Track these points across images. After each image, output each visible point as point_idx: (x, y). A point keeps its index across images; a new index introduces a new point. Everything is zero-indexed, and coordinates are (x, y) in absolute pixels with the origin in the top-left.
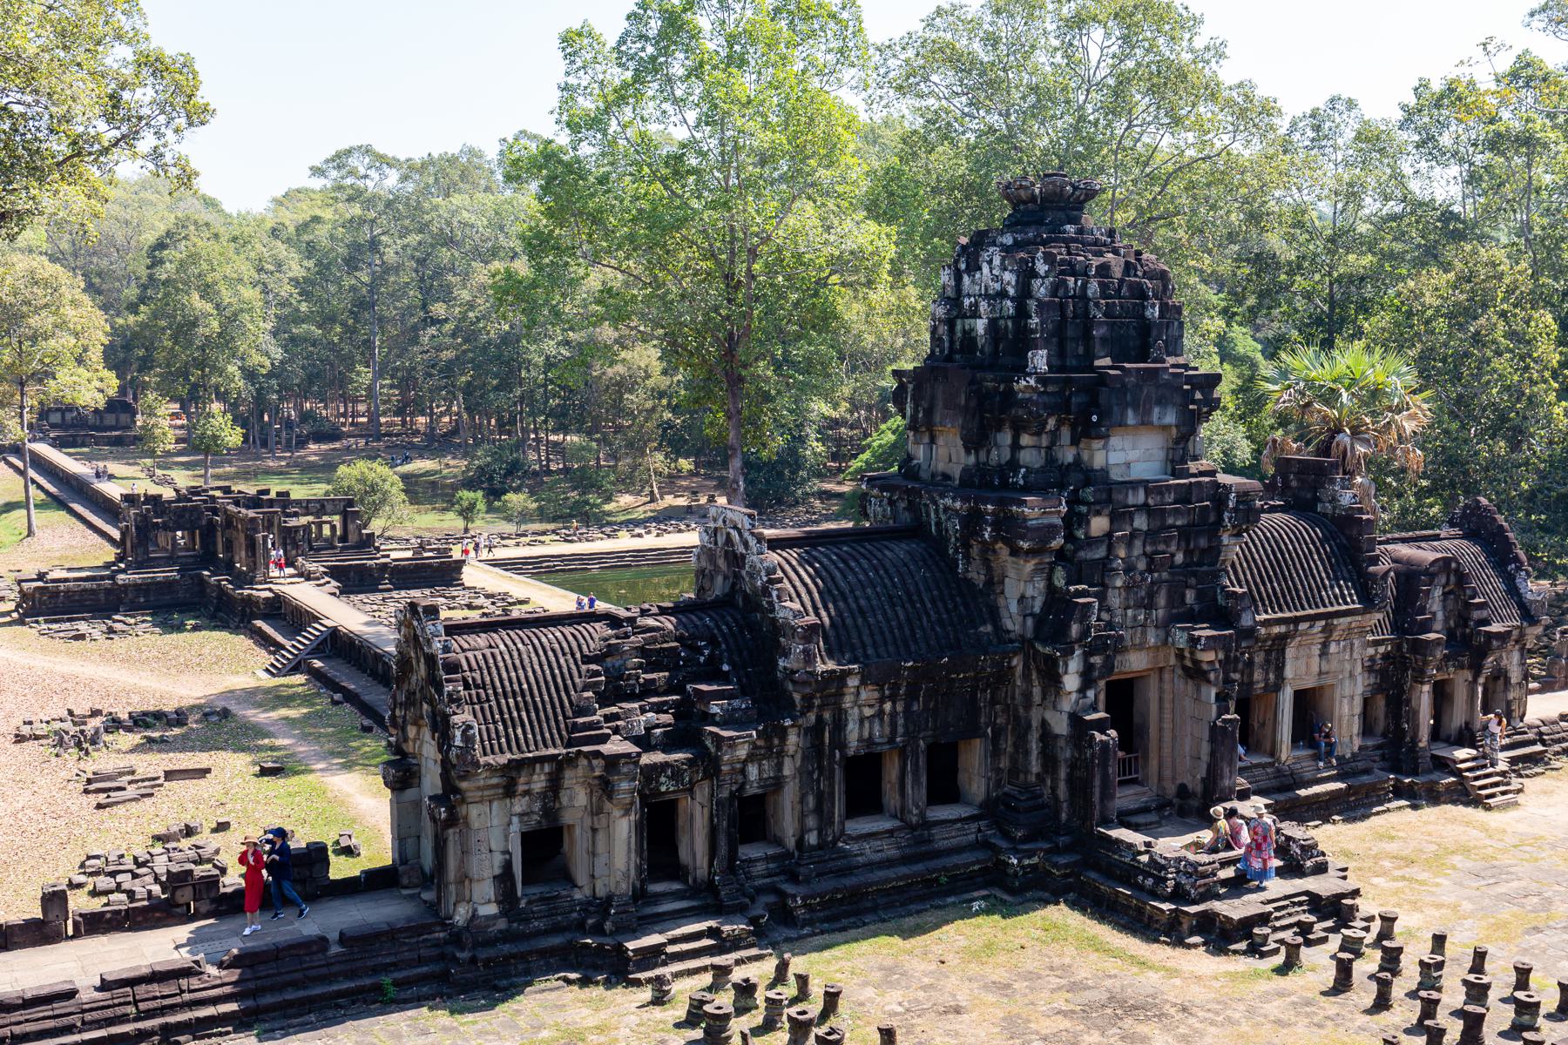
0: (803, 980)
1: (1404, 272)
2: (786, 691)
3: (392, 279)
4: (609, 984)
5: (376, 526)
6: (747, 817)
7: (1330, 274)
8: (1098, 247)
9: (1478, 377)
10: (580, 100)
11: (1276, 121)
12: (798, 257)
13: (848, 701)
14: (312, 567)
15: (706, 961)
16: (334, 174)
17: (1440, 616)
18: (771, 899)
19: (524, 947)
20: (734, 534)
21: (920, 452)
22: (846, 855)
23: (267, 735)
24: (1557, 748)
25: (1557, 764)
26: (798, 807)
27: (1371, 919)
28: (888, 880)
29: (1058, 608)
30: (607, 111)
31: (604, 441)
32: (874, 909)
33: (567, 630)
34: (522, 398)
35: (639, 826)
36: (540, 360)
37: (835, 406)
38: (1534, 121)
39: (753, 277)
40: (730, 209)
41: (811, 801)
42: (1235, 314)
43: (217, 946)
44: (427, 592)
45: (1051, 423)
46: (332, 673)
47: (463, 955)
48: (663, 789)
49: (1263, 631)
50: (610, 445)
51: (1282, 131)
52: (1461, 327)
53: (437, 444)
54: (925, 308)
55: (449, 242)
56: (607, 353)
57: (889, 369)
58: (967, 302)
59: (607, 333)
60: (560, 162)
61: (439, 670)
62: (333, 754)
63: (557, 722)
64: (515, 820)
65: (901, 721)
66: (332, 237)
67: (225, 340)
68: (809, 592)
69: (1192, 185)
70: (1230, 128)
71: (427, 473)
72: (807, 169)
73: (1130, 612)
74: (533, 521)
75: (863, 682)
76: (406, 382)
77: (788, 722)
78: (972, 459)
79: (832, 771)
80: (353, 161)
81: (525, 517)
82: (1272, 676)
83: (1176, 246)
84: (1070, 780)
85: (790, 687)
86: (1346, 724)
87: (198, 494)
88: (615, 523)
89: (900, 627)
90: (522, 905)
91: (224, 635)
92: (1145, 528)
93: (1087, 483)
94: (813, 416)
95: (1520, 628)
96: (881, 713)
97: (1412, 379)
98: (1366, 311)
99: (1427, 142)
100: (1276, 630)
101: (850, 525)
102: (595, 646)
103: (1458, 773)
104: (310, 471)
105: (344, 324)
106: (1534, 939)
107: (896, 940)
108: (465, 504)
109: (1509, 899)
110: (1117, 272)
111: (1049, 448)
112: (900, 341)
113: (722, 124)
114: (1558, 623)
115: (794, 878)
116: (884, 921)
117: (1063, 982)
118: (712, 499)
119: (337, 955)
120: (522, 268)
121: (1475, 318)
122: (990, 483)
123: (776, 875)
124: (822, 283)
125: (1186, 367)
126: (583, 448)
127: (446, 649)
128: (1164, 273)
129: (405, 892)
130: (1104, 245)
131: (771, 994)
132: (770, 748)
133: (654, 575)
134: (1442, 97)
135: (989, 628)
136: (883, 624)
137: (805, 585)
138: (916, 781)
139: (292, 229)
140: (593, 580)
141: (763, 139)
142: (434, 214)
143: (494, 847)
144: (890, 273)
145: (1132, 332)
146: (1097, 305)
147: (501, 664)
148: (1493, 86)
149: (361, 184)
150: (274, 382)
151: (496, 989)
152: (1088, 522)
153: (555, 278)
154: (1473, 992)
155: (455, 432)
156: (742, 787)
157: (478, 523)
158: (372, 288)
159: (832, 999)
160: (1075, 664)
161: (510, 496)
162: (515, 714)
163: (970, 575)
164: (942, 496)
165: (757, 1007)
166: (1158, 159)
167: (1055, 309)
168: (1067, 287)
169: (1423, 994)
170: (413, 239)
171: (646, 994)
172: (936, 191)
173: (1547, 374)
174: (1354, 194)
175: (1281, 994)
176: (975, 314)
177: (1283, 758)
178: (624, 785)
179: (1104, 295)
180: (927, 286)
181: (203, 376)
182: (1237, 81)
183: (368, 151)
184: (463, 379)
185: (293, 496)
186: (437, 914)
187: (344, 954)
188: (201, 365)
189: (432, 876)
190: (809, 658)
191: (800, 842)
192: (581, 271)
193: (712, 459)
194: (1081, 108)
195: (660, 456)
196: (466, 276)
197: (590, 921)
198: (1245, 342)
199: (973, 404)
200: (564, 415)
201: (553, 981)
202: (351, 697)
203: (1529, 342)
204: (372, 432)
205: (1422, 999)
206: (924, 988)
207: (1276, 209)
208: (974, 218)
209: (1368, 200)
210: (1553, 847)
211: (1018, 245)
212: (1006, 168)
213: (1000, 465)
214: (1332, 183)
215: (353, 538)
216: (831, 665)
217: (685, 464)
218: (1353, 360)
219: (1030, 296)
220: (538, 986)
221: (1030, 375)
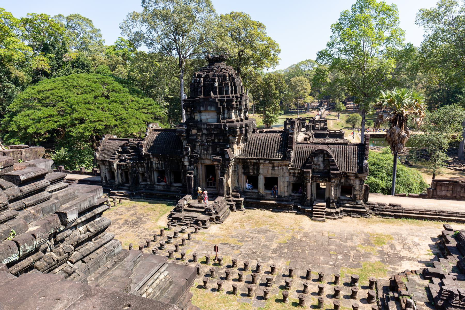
82: (255, 172)
86: (284, 188)
92: (206, 133)
100: (253, 161)
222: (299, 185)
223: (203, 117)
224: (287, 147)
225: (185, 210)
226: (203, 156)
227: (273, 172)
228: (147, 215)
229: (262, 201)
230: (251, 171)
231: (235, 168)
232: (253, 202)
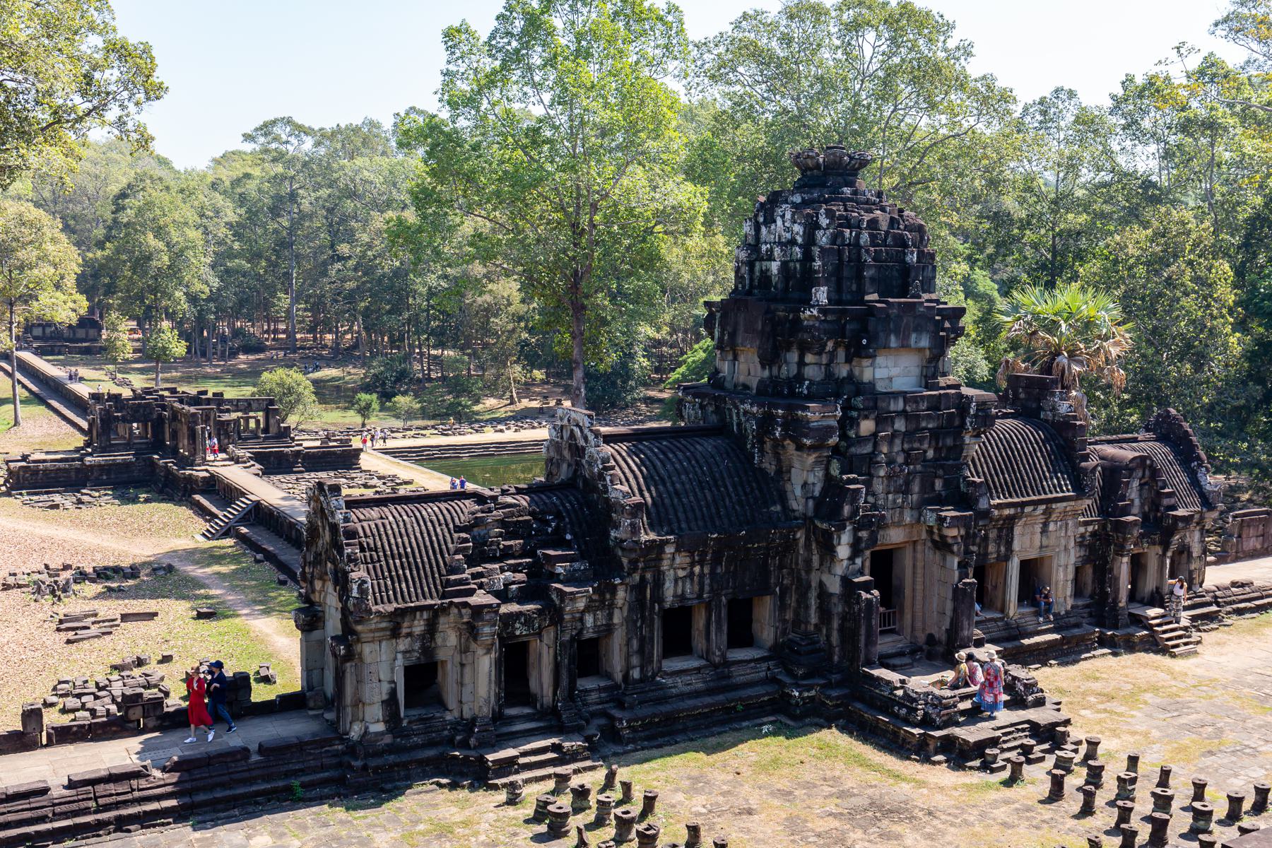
0: (627, 787)
1: (1112, 228)
2: (616, 556)
3: (307, 224)
4: (473, 788)
5: (292, 420)
6: (584, 656)
7: (1053, 229)
8: (869, 205)
9: (1169, 312)
10: (459, 83)
11: (1012, 107)
12: (630, 210)
13: (665, 565)
14: (240, 453)
15: (550, 770)
16: (262, 140)
17: (1137, 502)
18: (602, 721)
19: (405, 758)
20: (577, 430)
21: (725, 367)
22: (662, 687)
23: (203, 586)
24: (1228, 608)
25: (1228, 622)
26: (625, 649)
27: (1079, 743)
28: (696, 708)
29: (833, 493)
30: (479, 92)
31: (474, 355)
32: (684, 731)
33: (443, 506)
34: (409, 320)
35: (498, 663)
36: (424, 290)
37: (658, 330)
38: (1216, 110)
39: (594, 226)
40: (576, 172)
41: (635, 643)
42: (977, 260)
43: (161, 754)
44: (332, 474)
45: (830, 345)
46: (255, 538)
47: (357, 764)
48: (518, 633)
49: (996, 512)
50: (479, 358)
51: (1017, 115)
52: (1157, 273)
53: (340, 356)
54: (730, 252)
55: (353, 195)
56: (477, 285)
57: (702, 300)
58: (764, 248)
59: (478, 269)
60: (442, 132)
61: (340, 536)
62: (256, 602)
63: (434, 578)
64: (400, 656)
65: (707, 581)
66: (260, 190)
67: (174, 271)
68: (636, 477)
69: (943, 158)
70: (975, 112)
71: (333, 379)
72: (638, 141)
73: (890, 497)
74: (416, 419)
75: (678, 550)
76: (317, 306)
77: (618, 581)
78: (766, 373)
79: (652, 620)
80: (277, 130)
81: (410, 415)
82: (1003, 549)
83: (931, 206)
84: (841, 629)
85: (620, 553)
86: (1061, 587)
87: (150, 394)
88: (482, 421)
89: (708, 506)
90: (405, 724)
91: (170, 506)
93: (858, 394)
94: (641, 337)
95: (1201, 513)
96: (692, 574)
97: (1117, 313)
98: (1082, 259)
99: (1131, 125)
100: (1007, 512)
101: (669, 424)
102: (465, 518)
103: (1150, 628)
104: (240, 376)
105: (268, 260)
106: (1209, 761)
107: (701, 755)
108: (363, 404)
109: (1189, 728)
110: (884, 225)
111: (828, 365)
112: (711, 278)
113: (571, 104)
114: (1230, 509)
115: (621, 705)
116: (692, 740)
117: (834, 790)
118: (559, 403)
119: (257, 762)
120: (411, 216)
121: (1168, 266)
122: (781, 392)
123: (607, 702)
124: (649, 231)
125: (938, 302)
126: (457, 361)
127: (346, 520)
128: (921, 227)
129: (311, 713)
130: (874, 204)
131: (602, 797)
132: (602, 601)
133: (513, 462)
134: (1144, 89)
135: (778, 508)
136: (694, 504)
137: (633, 472)
138: (719, 629)
139: (227, 183)
140: (464, 465)
141: (603, 116)
142: (341, 173)
143: (382, 677)
144: (703, 224)
145: (895, 274)
146: (867, 251)
147: (390, 532)
148: (1184, 81)
149: (283, 148)
150: (212, 305)
151: (383, 791)
152: (858, 425)
153: (437, 225)
154: (1160, 802)
155: (355, 346)
156: (580, 632)
157: (373, 419)
158: (292, 230)
159: (650, 802)
160: (846, 538)
161: (399, 398)
162: (401, 572)
163: (763, 466)
164: (743, 403)
165: (590, 808)
166: (918, 136)
167: (834, 255)
168: (843, 236)
169: (1120, 803)
170: (324, 192)
171: (502, 796)
172: (740, 159)
173: (1224, 311)
174: (1072, 166)
175: (1007, 802)
176: (770, 258)
177: (1011, 614)
178: (487, 630)
179: (873, 244)
180: (732, 235)
181: (156, 299)
182: (981, 75)
183: (289, 121)
184: (363, 304)
185: (226, 396)
186: (336, 730)
187: (261, 762)
188: (154, 290)
189: (333, 701)
190: (635, 530)
191: (626, 676)
192: (458, 220)
193: (560, 370)
194: (857, 94)
195: (518, 368)
196: (366, 222)
197: (458, 738)
198: (984, 282)
199: (768, 329)
200: (443, 334)
201: (428, 785)
202: (270, 557)
203: (1210, 285)
204: (290, 346)
205: (1119, 807)
206: (724, 794)
207: (1011, 177)
208: (771, 181)
209: (1084, 171)
210: (1225, 687)
211: (805, 203)
212: (796, 142)
213: (788, 378)
214: (1055, 157)
215: (273, 430)
216: (653, 536)
217: (539, 374)
218: (1071, 297)
219: (815, 244)
220: (416, 789)
221: (813, 306)
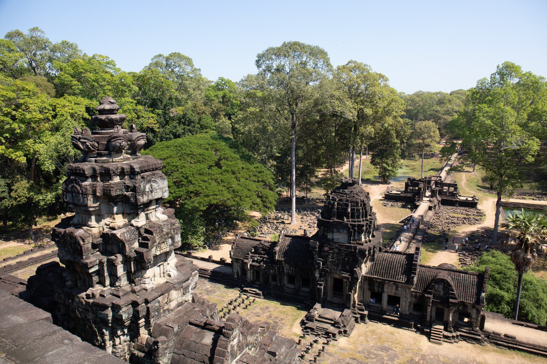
222: (420, 304)
223: (335, 237)
224: (411, 272)
225: (316, 320)
226: (332, 271)
227: (397, 292)
228: (282, 319)
229: (385, 316)
230: (376, 288)
231: (361, 284)
232: (377, 316)
